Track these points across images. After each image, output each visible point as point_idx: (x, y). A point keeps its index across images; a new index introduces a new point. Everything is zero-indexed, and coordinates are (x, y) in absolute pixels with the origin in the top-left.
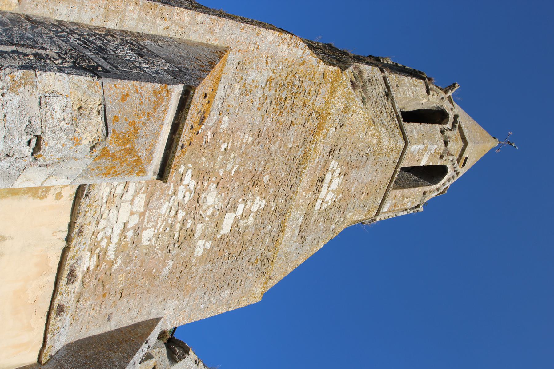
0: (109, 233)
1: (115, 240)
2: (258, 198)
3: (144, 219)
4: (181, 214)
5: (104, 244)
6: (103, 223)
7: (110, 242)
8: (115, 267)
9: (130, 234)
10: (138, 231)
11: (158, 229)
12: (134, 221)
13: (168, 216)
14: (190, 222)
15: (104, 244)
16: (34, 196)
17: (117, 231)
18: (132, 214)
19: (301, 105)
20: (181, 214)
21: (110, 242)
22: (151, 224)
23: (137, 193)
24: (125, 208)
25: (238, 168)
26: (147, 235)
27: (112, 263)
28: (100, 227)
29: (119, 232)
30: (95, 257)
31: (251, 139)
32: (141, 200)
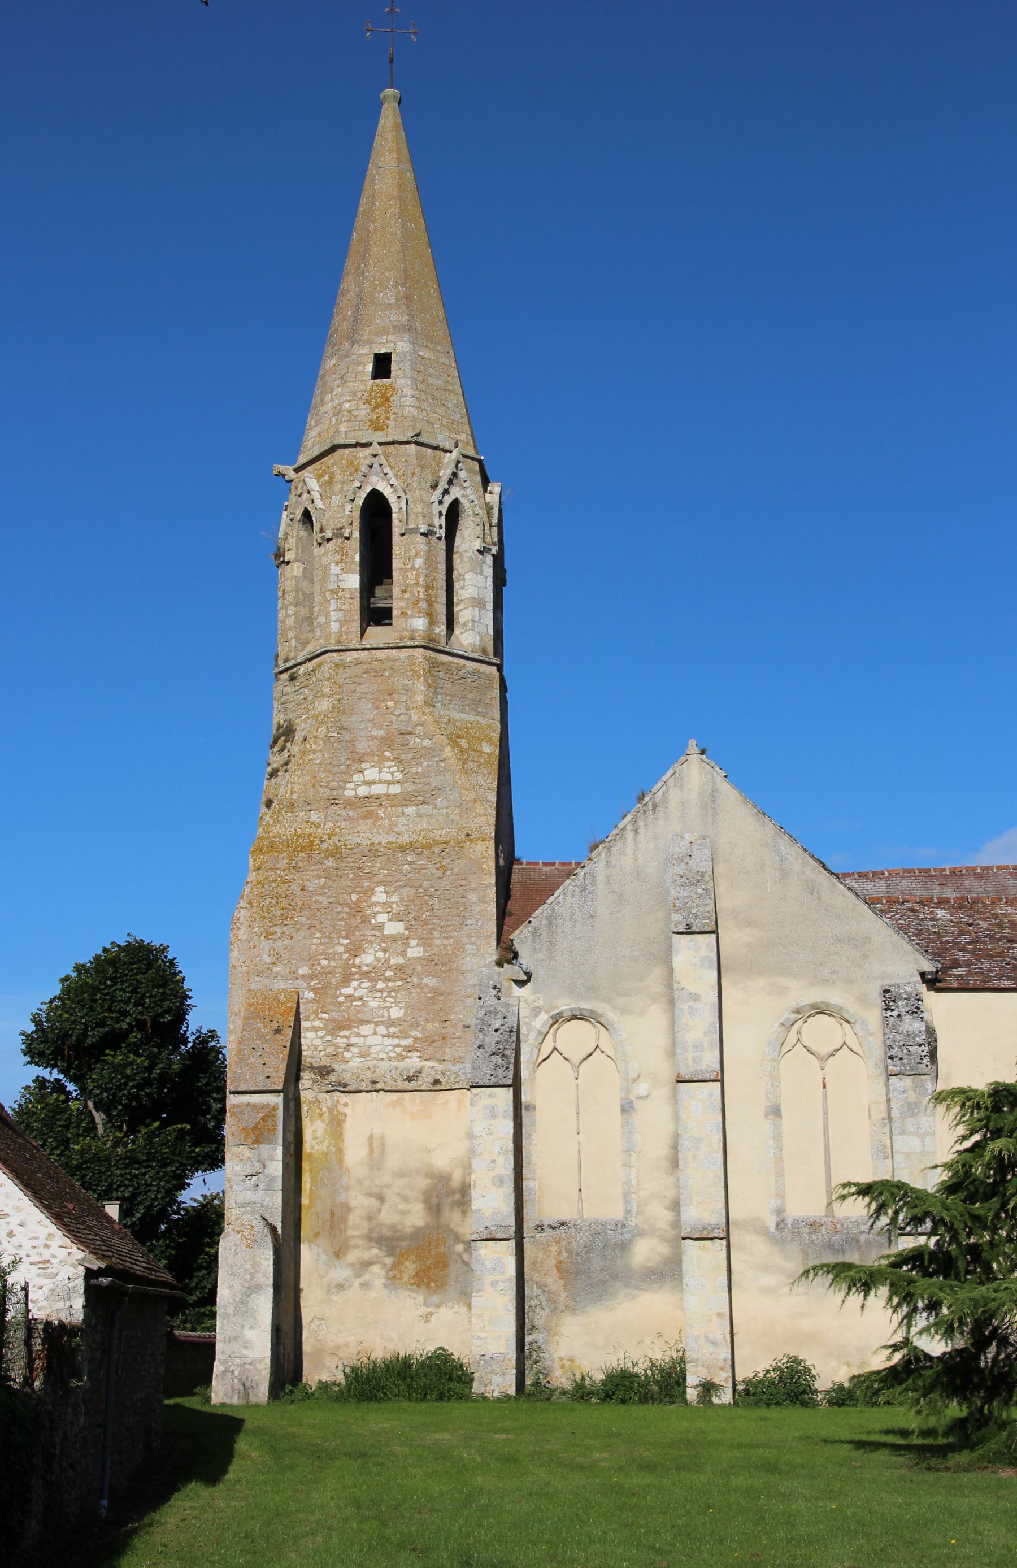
0: (390, 1048)
1: (396, 1041)
2: (374, 899)
3: (381, 1022)
4: (380, 985)
5: (398, 1050)
6: (382, 1055)
7: (398, 1046)
8: (419, 1035)
9: (392, 1030)
10: (390, 1023)
11: (392, 1003)
12: (382, 1030)
13: (381, 997)
14: (389, 973)
15: (398, 1050)
16: (344, 1121)
17: (388, 1041)
18: (375, 1033)
19: (285, 886)
20: (380, 985)
21: (398, 1046)
22: (386, 1014)
23: (358, 1035)
24: (369, 1041)
25: (342, 938)
26: (396, 1013)
27: (416, 1040)
28: (384, 1056)
29: (390, 1039)
30: (409, 1054)
31: (318, 935)
32: (365, 1029)
